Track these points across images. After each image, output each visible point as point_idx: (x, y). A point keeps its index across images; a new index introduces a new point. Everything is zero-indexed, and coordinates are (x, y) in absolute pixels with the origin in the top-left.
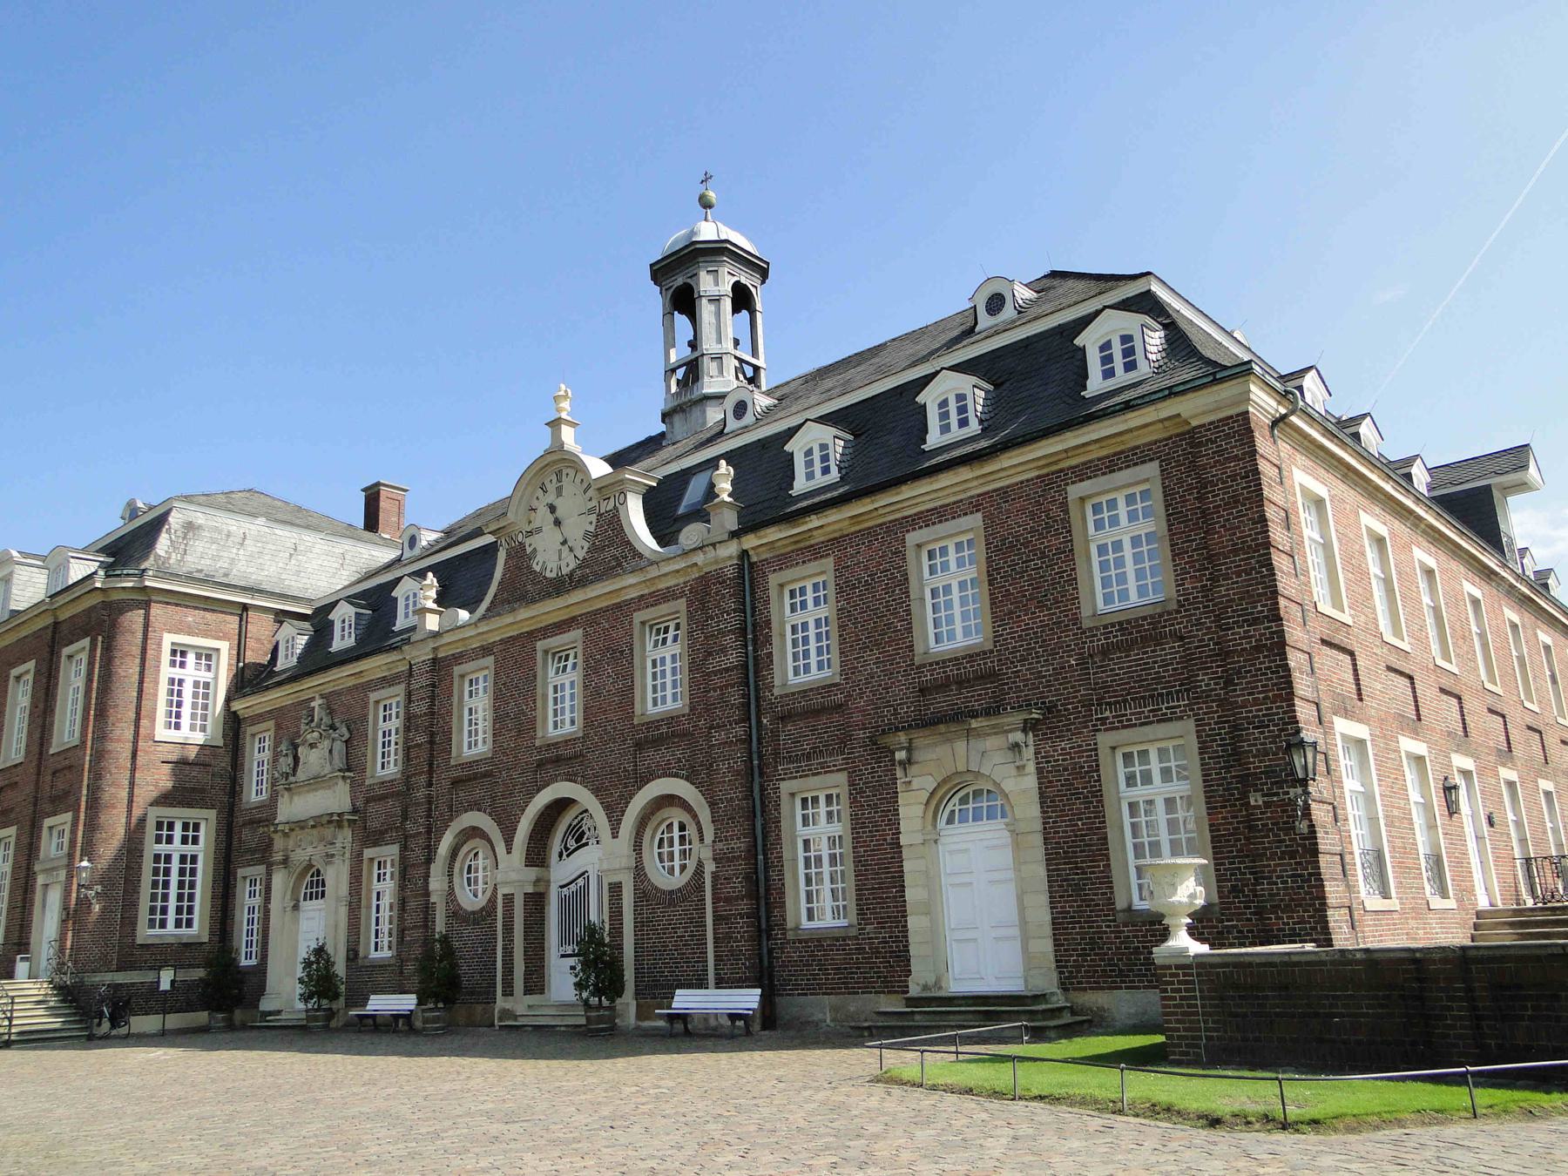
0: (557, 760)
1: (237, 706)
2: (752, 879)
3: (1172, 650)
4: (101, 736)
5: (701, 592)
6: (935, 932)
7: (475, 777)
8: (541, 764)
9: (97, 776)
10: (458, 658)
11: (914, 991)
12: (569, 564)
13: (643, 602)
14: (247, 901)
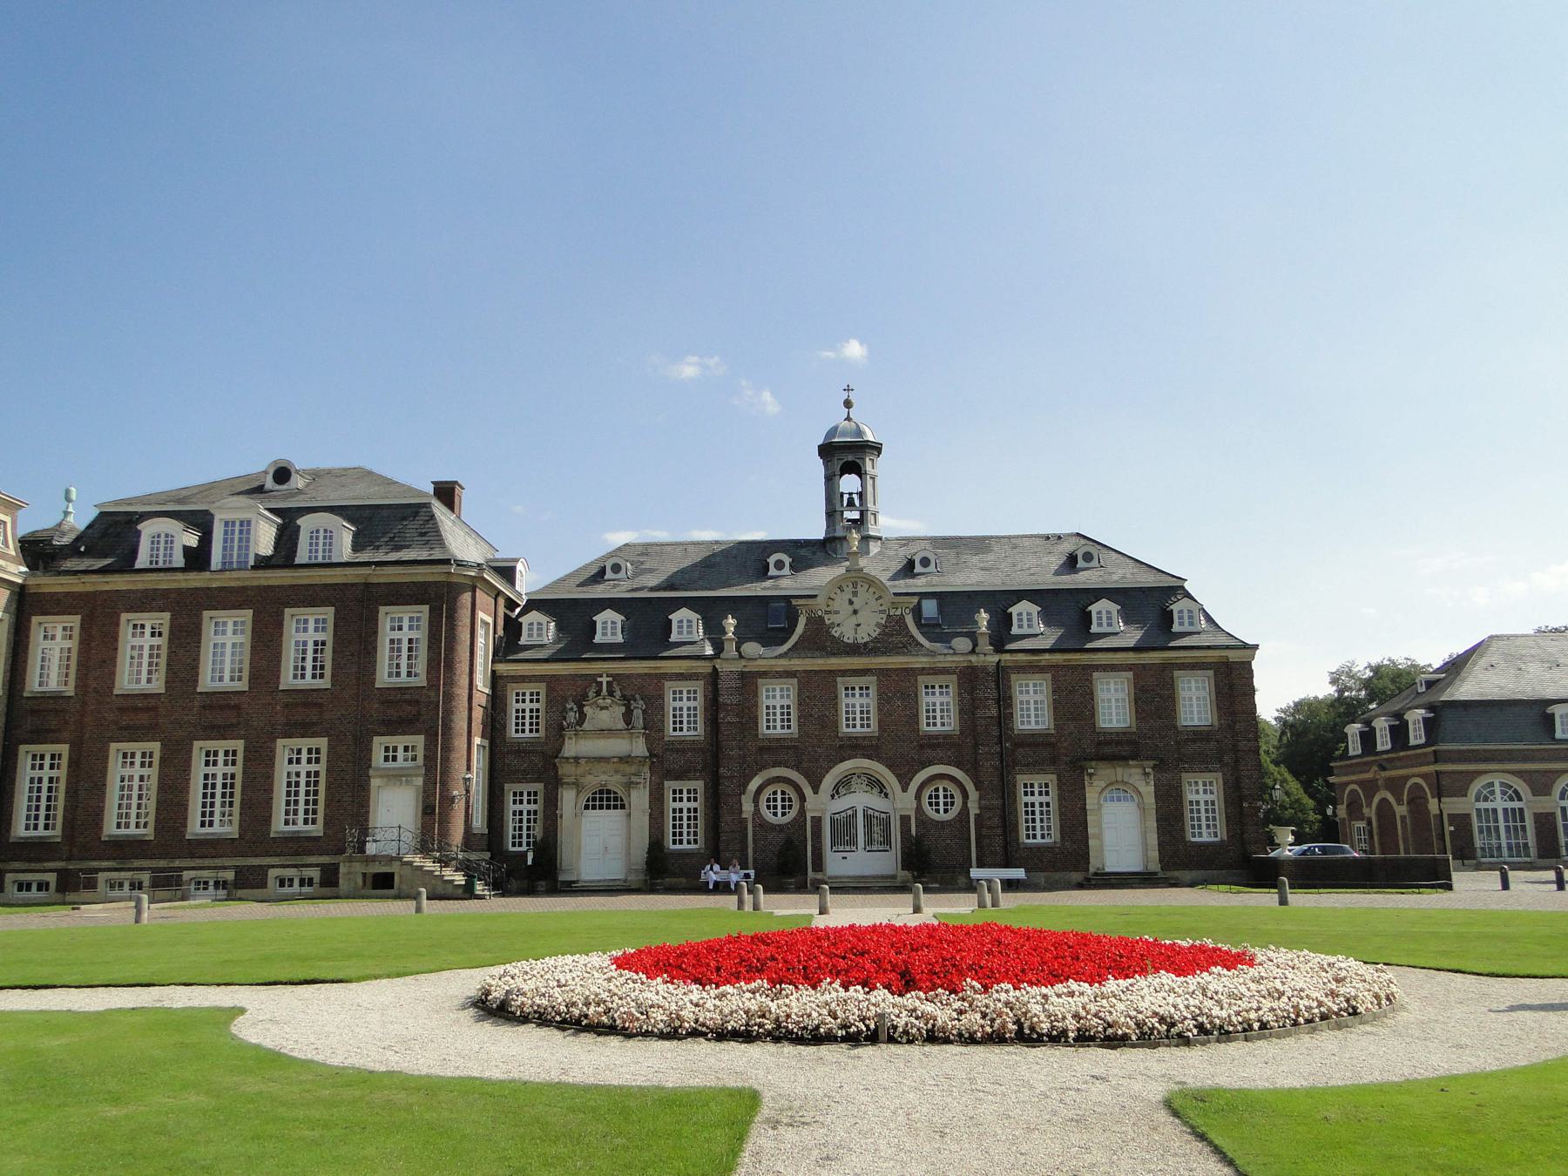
1: (502, 668)
2: (1004, 819)
3: (1213, 744)
4: (450, 683)
6: (1101, 849)
7: (783, 747)
8: (841, 747)
9: (449, 712)
10: (764, 674)
11: (1092, 870)
12: (863, 636)
13: (923, 671)
14: (520, 806)
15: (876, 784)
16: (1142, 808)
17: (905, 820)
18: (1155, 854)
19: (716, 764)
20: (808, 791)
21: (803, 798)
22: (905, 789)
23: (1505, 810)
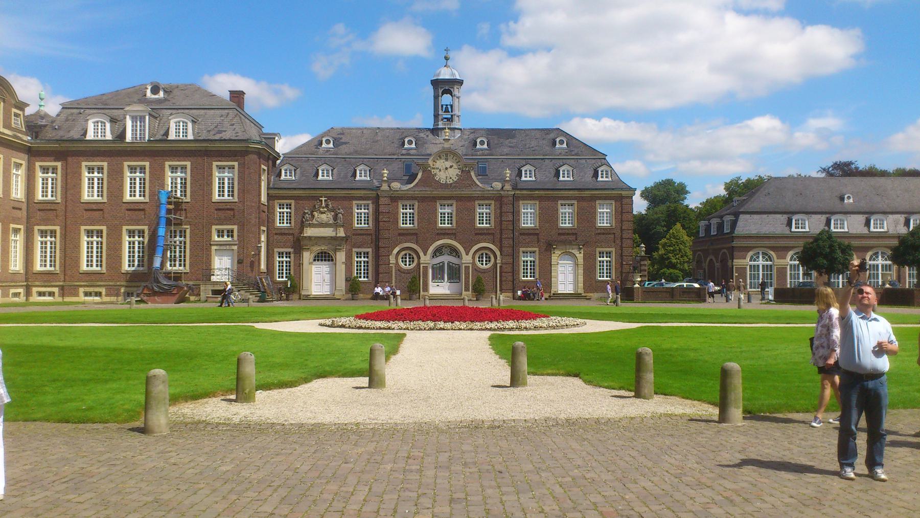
0: (444, 234)
5: (499, 199)
12: (450, 181)
15: (454, 252)
16: (576, 265)
17: (467, 268)
18: (581, 285)
19: (377, 239)
20: (421, 254)
21: (419, 258)
22: (467, 254)
23: (763, 266)
